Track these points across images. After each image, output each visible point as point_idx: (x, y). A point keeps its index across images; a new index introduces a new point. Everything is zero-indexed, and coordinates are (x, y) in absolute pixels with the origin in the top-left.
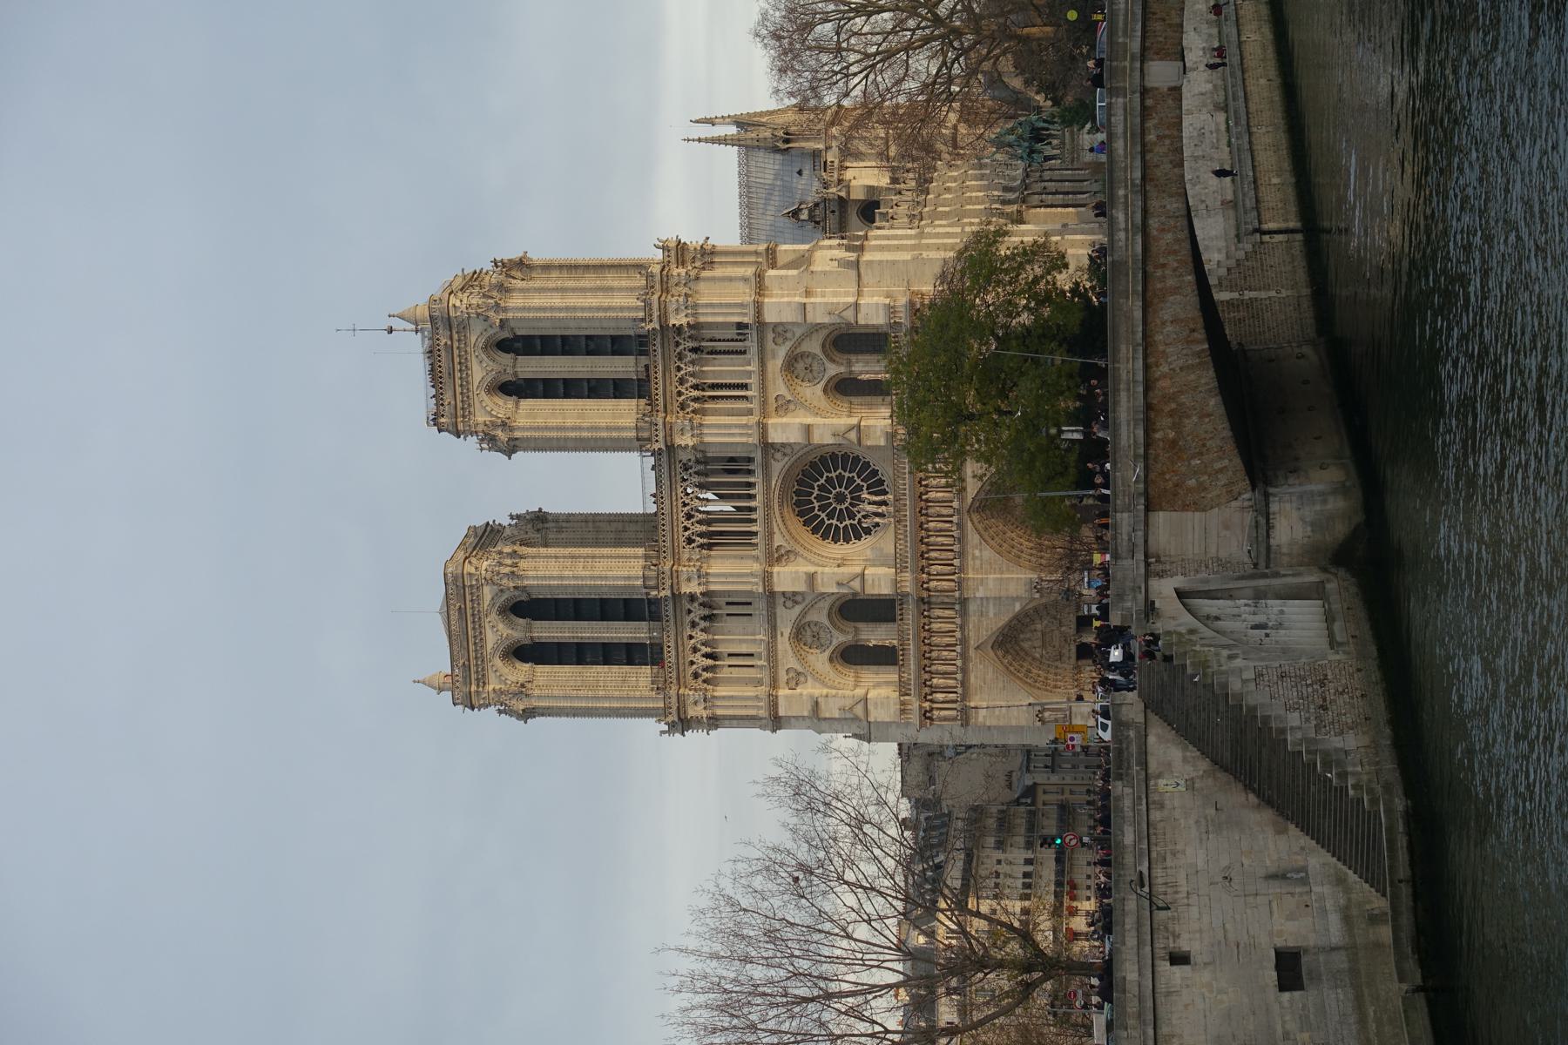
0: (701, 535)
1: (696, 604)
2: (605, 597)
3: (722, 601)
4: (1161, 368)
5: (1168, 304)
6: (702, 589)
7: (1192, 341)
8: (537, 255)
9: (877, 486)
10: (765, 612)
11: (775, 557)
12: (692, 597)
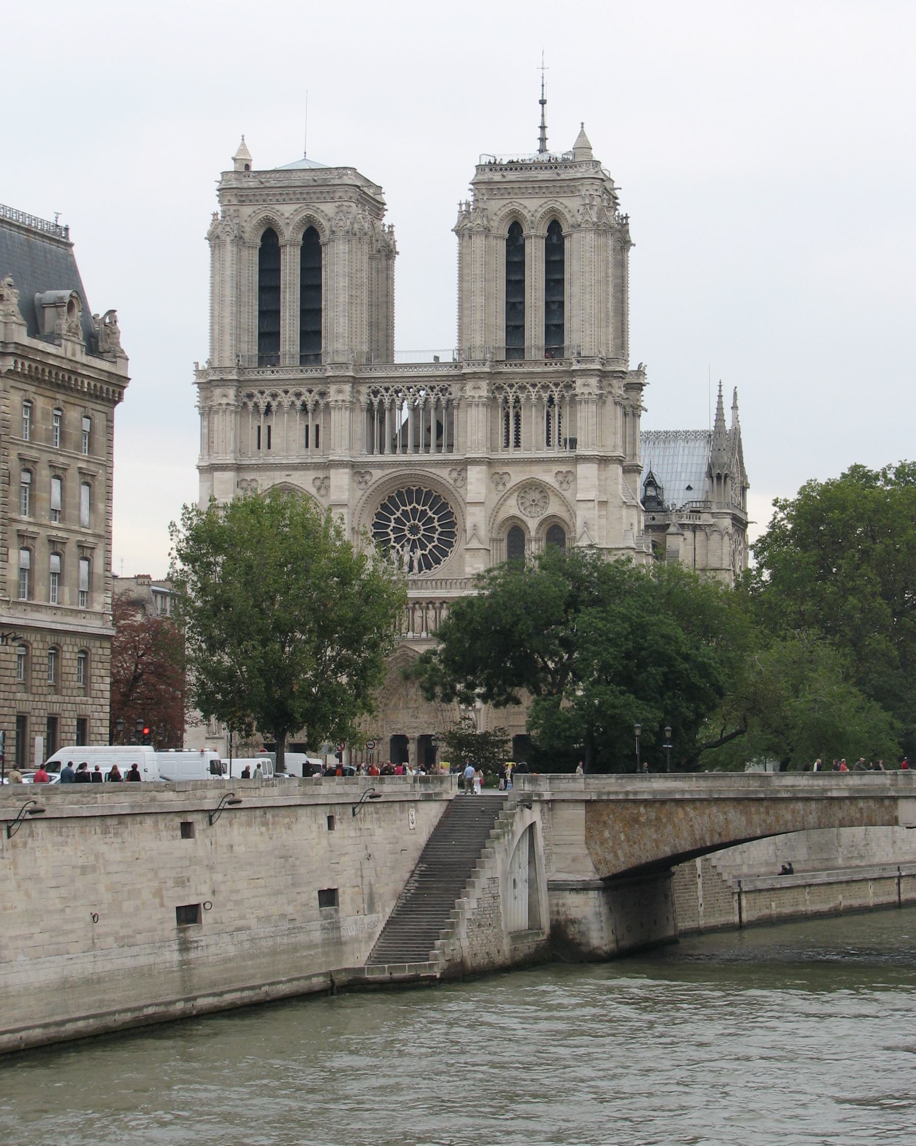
0: (381, 403)
1: (317, 397)
2: (323, 314)
3: (320, 421)
6: (332, 404)
8: (633, 255)
9: (427, 563)
10: (309, 461)
11: (358, 470)
12: (323, 394)
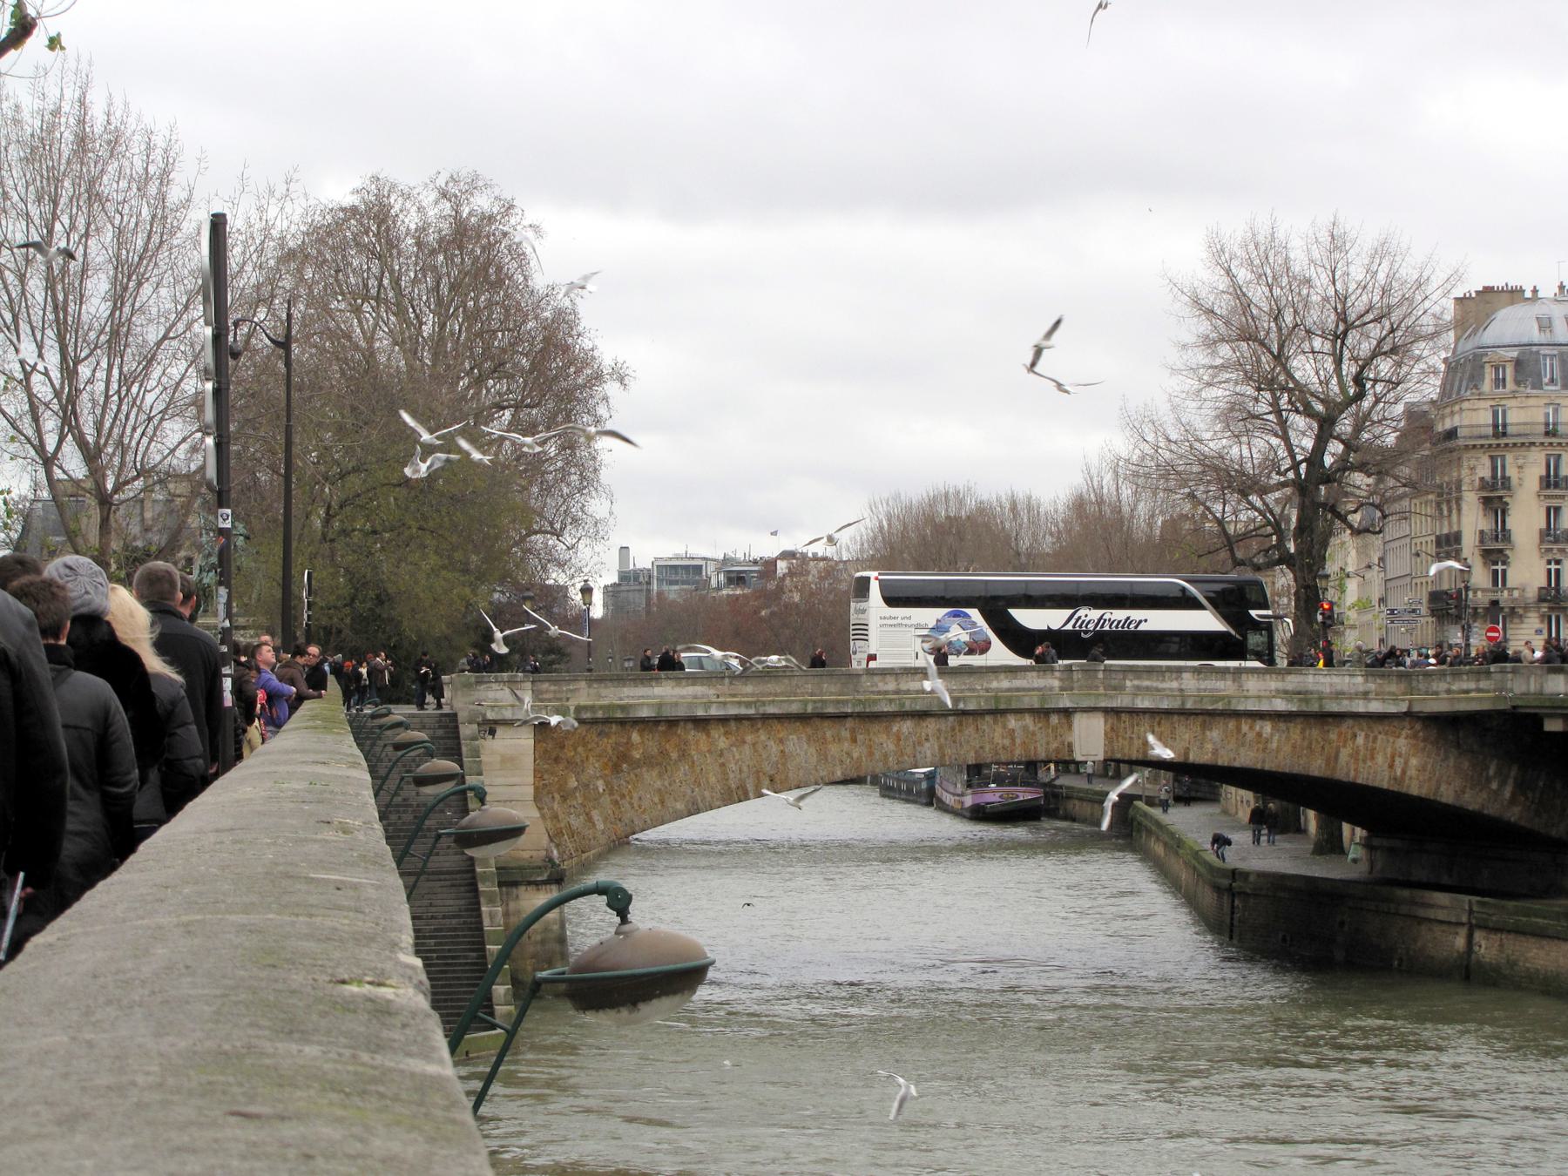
5: (805, 746)
7: (758, 778)
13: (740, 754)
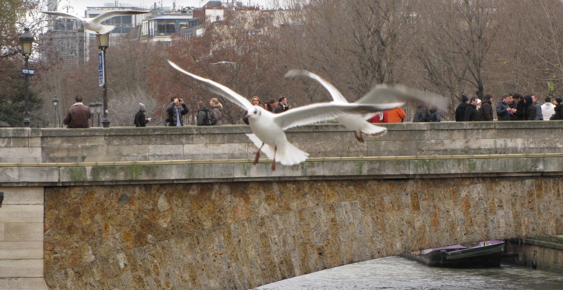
4: (264, 205)
5: (360, 214)
13: (285, 221)
